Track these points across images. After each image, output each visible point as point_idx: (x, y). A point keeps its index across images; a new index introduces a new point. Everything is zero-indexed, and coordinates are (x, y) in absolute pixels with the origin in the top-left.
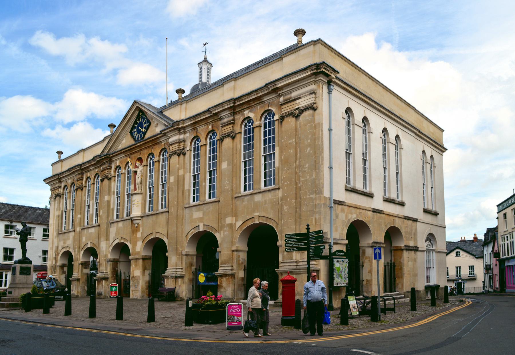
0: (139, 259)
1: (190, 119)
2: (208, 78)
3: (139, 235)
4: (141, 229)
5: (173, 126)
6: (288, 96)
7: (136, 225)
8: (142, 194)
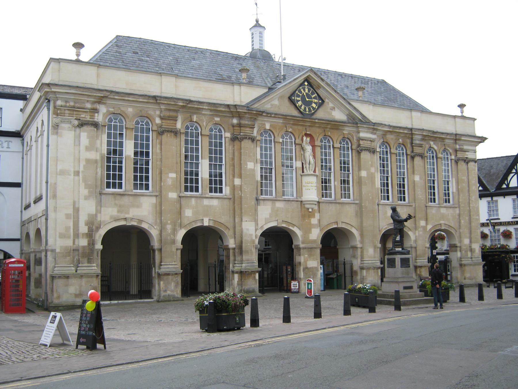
0: (315, 248)
1: (390, 126)
2: (260, 44)
3: (314, 221)
4: (317, 215)
5: (374, 126)
6: (462, 147)
7: (310, 210)
8: (317, 176)
